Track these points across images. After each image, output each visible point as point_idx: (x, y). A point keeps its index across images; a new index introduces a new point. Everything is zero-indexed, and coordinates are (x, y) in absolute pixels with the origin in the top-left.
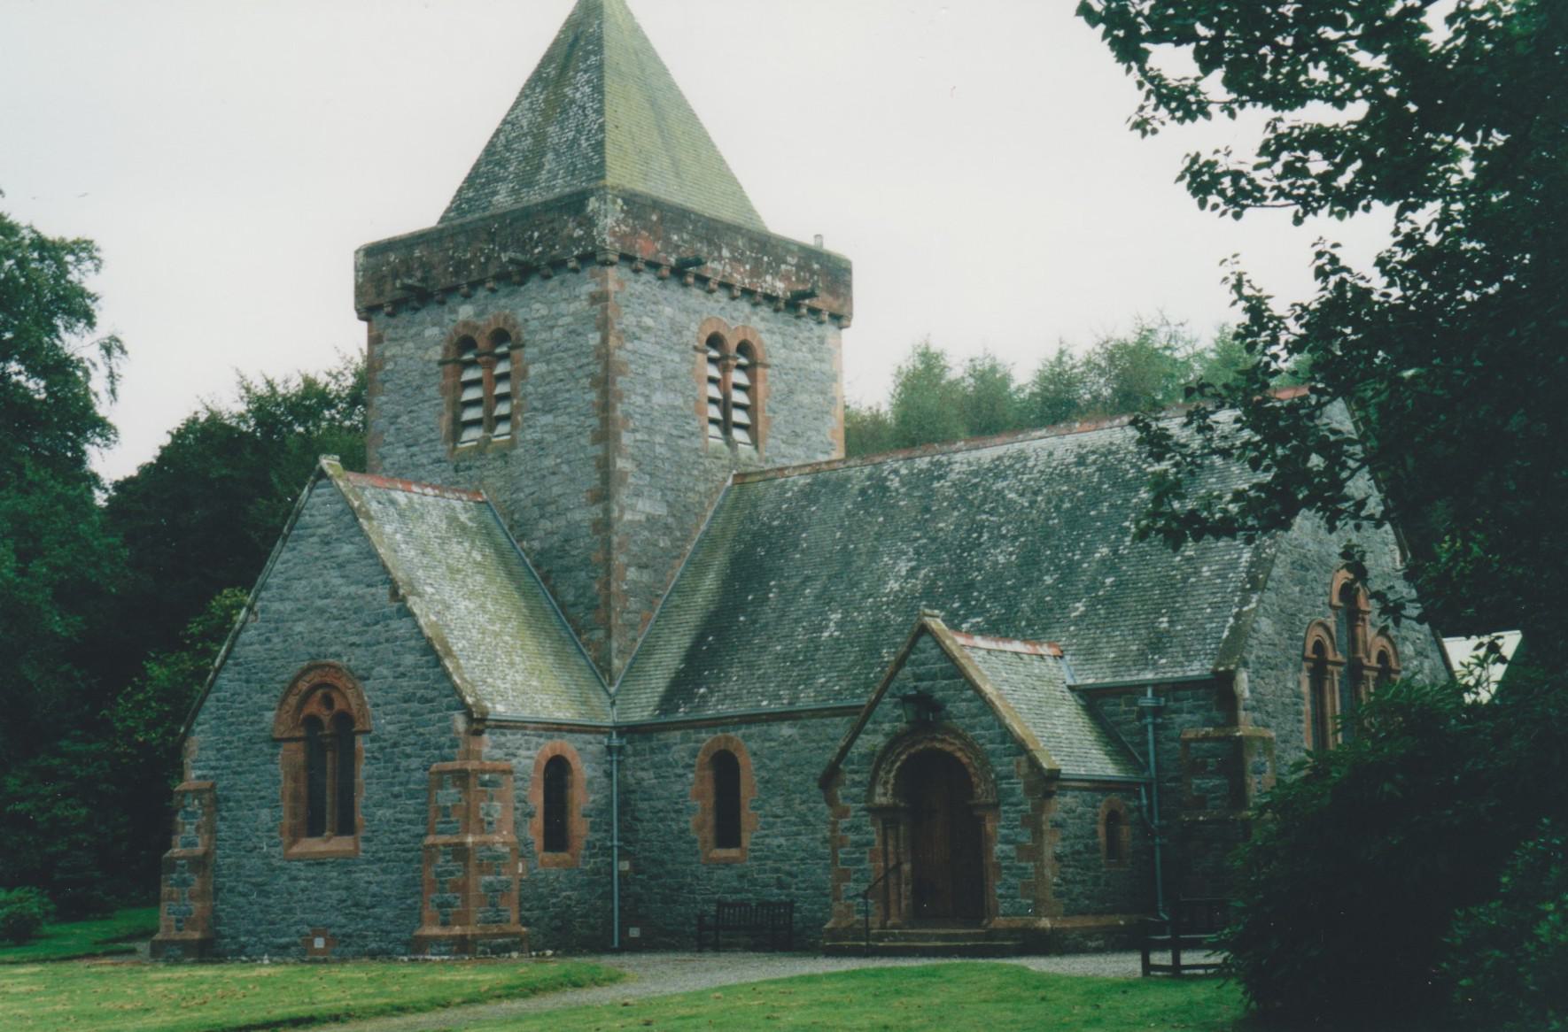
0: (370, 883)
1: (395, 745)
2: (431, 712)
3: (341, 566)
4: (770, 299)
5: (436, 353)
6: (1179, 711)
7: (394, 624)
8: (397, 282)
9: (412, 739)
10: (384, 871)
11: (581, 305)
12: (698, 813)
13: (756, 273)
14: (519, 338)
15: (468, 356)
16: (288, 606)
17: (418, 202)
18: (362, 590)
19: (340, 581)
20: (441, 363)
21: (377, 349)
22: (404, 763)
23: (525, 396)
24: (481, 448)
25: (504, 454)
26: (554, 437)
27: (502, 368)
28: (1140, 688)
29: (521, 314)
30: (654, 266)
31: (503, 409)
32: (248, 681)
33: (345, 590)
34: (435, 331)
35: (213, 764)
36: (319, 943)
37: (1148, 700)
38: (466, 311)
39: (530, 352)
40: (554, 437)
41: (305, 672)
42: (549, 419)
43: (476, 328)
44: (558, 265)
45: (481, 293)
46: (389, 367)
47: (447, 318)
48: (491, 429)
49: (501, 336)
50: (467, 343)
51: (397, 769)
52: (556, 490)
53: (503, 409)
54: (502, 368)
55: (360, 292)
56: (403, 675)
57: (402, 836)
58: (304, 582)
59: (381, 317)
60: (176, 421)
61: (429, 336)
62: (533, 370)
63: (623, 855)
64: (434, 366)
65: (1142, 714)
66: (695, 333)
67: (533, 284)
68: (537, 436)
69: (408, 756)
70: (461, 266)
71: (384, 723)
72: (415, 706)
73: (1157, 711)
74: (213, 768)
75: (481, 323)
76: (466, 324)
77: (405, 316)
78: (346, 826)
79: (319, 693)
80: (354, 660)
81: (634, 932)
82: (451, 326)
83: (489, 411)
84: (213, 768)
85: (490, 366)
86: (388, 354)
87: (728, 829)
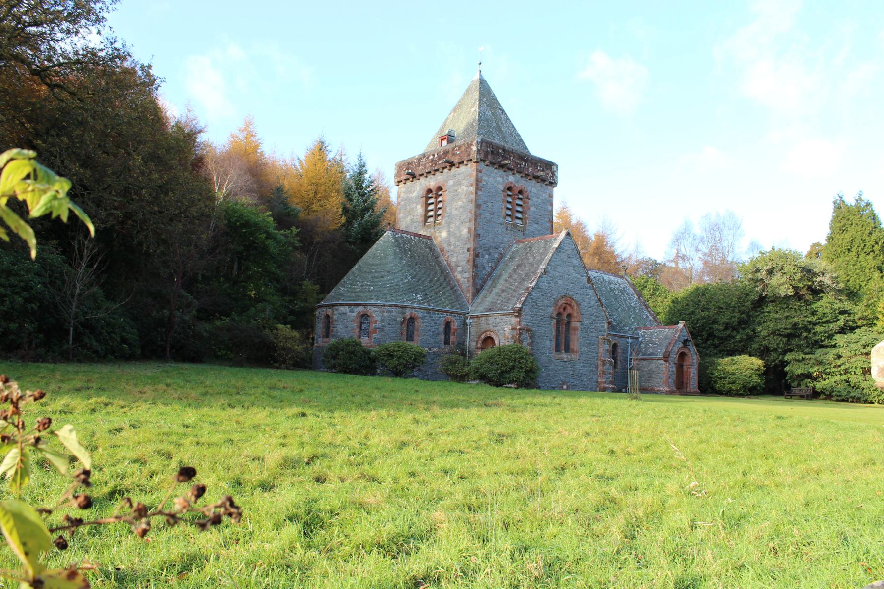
16: (557, 274)
18: (579, 276)
29: (529, 189)
33: (575, 275)
36: (565, 387)
38: (511, 178)
39: (530, 202)
42: (536, 226)
44: (543, 180)
45: (518, 176)
47: (505, 177)
62: (532, 209)
72: (594, 317)
77: (491, 169)
78: (567, 350)
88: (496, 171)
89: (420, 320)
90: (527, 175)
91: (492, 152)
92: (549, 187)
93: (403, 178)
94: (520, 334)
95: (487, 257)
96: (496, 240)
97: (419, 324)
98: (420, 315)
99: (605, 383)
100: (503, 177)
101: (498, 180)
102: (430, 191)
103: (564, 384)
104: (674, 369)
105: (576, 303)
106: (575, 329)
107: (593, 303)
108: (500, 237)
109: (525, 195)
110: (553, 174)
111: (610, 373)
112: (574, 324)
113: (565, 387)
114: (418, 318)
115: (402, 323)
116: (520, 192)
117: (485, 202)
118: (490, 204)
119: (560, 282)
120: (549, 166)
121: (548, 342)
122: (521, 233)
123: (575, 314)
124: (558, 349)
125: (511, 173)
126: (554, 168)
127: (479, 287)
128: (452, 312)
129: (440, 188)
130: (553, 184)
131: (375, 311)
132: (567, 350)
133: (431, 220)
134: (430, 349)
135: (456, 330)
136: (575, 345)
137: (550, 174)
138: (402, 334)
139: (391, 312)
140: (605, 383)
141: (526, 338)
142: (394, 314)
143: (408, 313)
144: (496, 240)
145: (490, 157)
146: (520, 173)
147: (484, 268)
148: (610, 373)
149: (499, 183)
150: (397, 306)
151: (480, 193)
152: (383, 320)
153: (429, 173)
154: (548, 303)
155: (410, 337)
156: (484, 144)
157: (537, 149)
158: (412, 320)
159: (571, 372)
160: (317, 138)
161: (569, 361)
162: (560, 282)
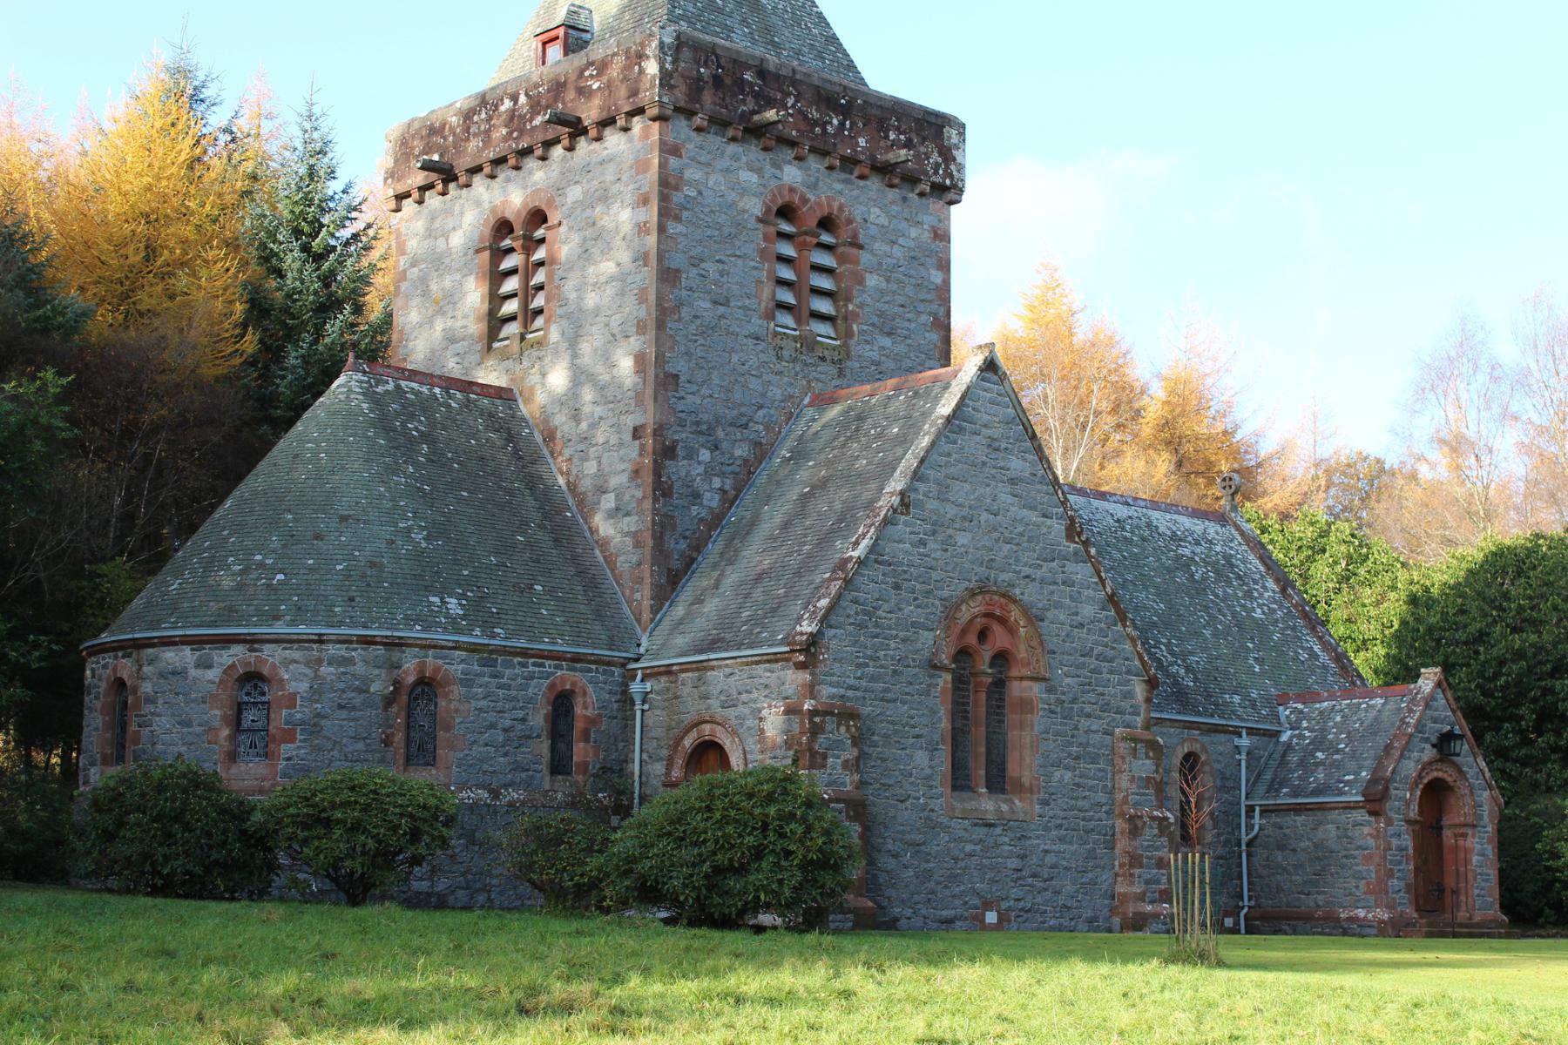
0: (1046, 851)
1: (1074, 701)
2: (1111, 672)
3: (1012, 481)
7: (1071, 567)
9: (1092, 697)
10: (1062, 840)
14: (855, 236)
16: (951, 511)
18: (1034, 517)
19: (1010, 499)
20: (760, 220)
21: (673, 162)
23: (861, 306)
29: (858, 212)
32: (897, 587)
35: (851, 681)
36: (991, 917)
38: (792, 174)
39: (865, 257)
41: (973, 594)
42: (886, 342)
43: (805, 200)
44: (911, 180)
45: (815, 164)
47: (769, 170)
51: (1076, 728)
56: (1082, 625)
57: (1081, 803)
58: (967, 486)
60: (406, 119)
62: (872, 281)
64: (752, 223)
68: (875, 355)
69: (1088, 716)
72: (1092, 662)
74: (850, 687)
77: (714, 140)
78: (998, 782)
82: (773, 183)
84: (850, 687)
86: (688, 174)
88: (733, 148)
89: (457, 691)
90: (849, 163)
91: (717, 81)
92: (934, 205)
93: (420, 178)
94: (815, 731)
95: (705, 455)
96: (737, 396)
97: (452, 702)
98: (457, 669)
99: (1141, 897)
100: (759, 171)
101: (741, 180)
102: (503, 227)
103: (987, 906)
104: (1408, 841)
105: (1025, 611)
106: (1026, 706)
107: (1088, 611)
108: (754, 383)
109: (845, 233)
110: (948, 155)
112: (1018, 689)
113: (991, 917)
114: (448, 681)
115: (389, 701)
116: (826, 223)
117: (696, 262)
118: (711, 268)
119: (963, 539)
120: (933, 132)
121: (921, 758)
122: (833, 370)
123: (1022, 653)
124: (960, 781)
125: (790, 153)
126: (951, 134)
127: (676, 564)
128: (576, 658)
129: (538, 217)
130: (948, 191)
131: (288, 662)
133: (512, 329)
134: (495, 794)
135: (592, 721)
136: (1024, 764)
137: (935, 157)
138: (387, 742)
139: (349, 661)
140: (1141, 897)
141: (837, 745)
142: (359, 668)
143: (410, 665)
144: (737, 396)
145: (708, 98)
146: (824, 154)
147: (696, 496)
149: (744, 192)
150: (368, 641)
151: (674, 228)
152: (316, 693)
153: (500, 161)
154: (918, 615)
155: (421, 750)
156: (686, 53)
157: (889, 68)
158: (427, 687)
159: (1013, 863)
160: (166, 57)
161: (1005, 822)
162: (963, 539)
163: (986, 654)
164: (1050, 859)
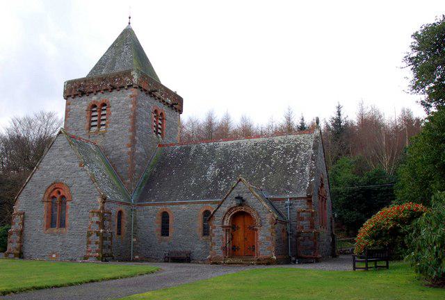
4: (167, 103)
5: (85, 108)
6: (296, 205)
8: (75, 90)
11: (128, 98)
12: (156, 226)
13: (165, 97)
15: (95, 109)
16: (49, 167)
17: (82, 70)
22: (82, 210)
24: (96, 132)
25: (103, 134)
26: (117, 130)
27: (103, 112)
28: (286, 199)
29: (110, 99)
30: (145, 90)
31: (103, 123)
34: (85, 102)
37: (288, 202)
38: (95, 98)
39: (112, 109)
40: (117, 130)
41: (52, 184)
42: (116, 125)
45: (99, 93)
46: (71, 111)
48: (99, 127)
49: (104, 105)
50: (94, 106)
52: (117, 144)
53: (103, 123)
54: (103, 112)
55: (65, 92)
59: (70, 99)
61: (83, 103)
63: (135, 237)
65: (286, 205)
66: (152, 109)
67: (114, 92)
70: (95, 87)
71: (76, 199)
72: (85, 195)
73: (290, 205)
75: (98, 101)
76: (94, 101)
77: (77, 98)
79: (56, 190)
80: (68, 182)
81: (137, 257)
83: (99, 123)
85: (100, 112)
87: (165, 231)
107: (84, 183)
111: (96, 243)
112: (68, 203)
116: (104, 105)
122: (101, 136)
125: (92, 94)
132: (63, 225)
136: (68, 221)
140: (90, 251)
146: (100, 91)
148: (96, 243)
159: (61, 243)
163: (58, 196)
164: (70, 242)
